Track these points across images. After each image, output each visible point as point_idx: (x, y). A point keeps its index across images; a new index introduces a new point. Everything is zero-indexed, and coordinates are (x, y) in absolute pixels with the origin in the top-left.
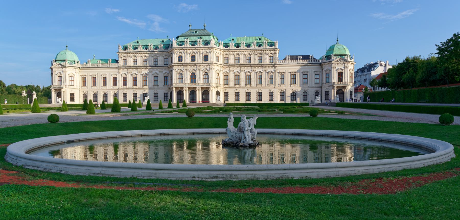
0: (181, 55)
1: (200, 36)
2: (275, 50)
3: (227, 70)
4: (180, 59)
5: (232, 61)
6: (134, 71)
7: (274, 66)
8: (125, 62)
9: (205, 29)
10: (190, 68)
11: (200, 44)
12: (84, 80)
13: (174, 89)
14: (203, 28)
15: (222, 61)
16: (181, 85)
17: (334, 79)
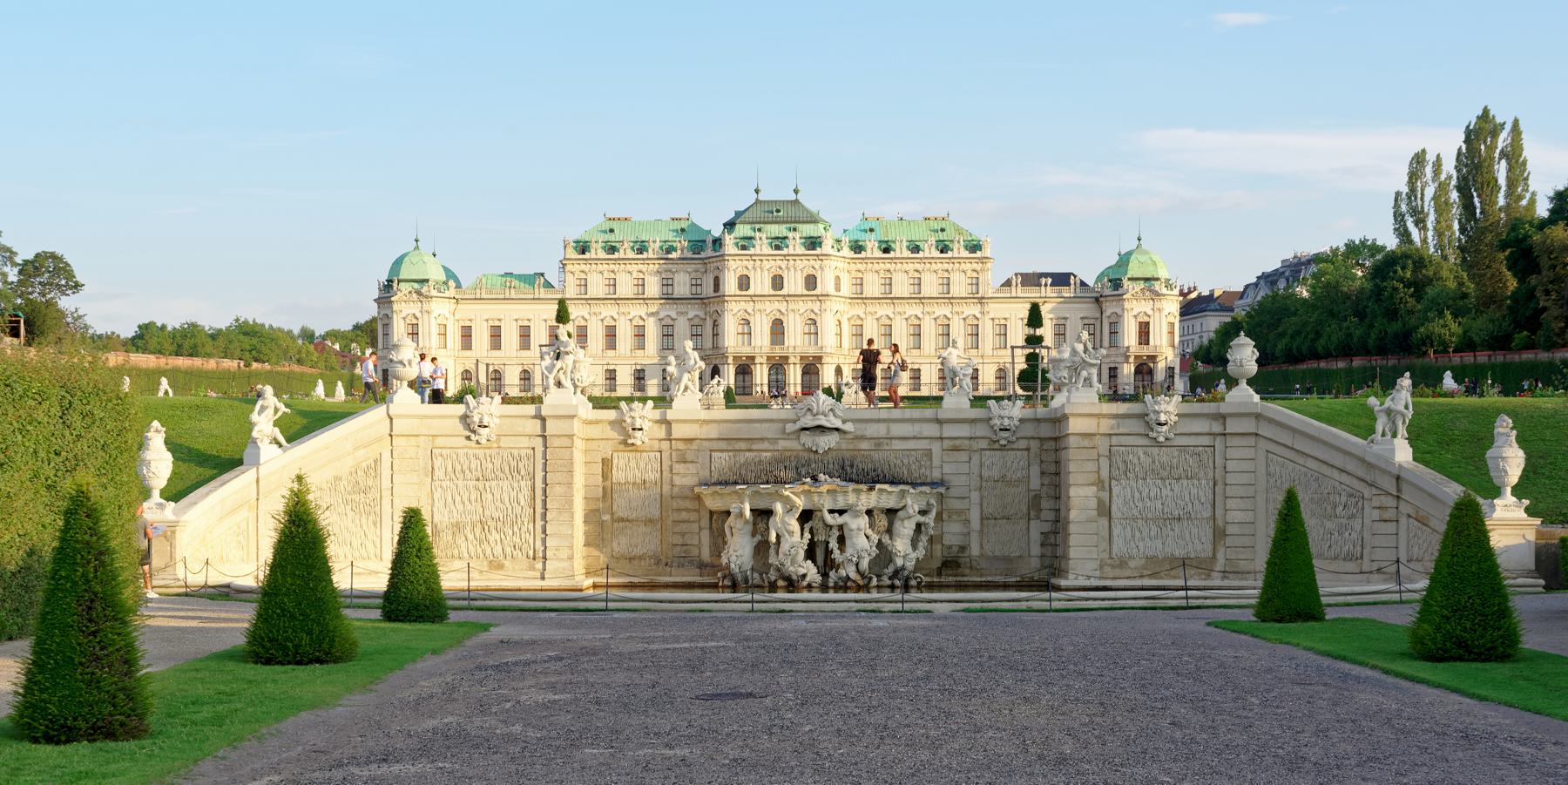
0: (745, 272)
1: (793, 222)
2: (983, 260)
3: (859, 310)
4: (744, 282)
5: (873, 287)
6: (608, 311)
7: (981, 300)
8: (585, 285)
9: (796, 202)
10: (772, 308)
11: (796, 246)
12: (467, 335)
13: (730, 360)
14: (793, 197)
15: (846, 289)
16: (746, 350)
17: (1130, 338)
